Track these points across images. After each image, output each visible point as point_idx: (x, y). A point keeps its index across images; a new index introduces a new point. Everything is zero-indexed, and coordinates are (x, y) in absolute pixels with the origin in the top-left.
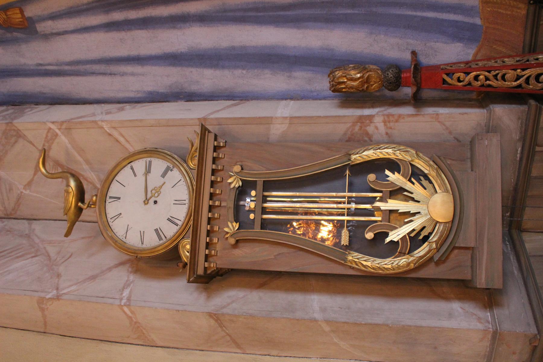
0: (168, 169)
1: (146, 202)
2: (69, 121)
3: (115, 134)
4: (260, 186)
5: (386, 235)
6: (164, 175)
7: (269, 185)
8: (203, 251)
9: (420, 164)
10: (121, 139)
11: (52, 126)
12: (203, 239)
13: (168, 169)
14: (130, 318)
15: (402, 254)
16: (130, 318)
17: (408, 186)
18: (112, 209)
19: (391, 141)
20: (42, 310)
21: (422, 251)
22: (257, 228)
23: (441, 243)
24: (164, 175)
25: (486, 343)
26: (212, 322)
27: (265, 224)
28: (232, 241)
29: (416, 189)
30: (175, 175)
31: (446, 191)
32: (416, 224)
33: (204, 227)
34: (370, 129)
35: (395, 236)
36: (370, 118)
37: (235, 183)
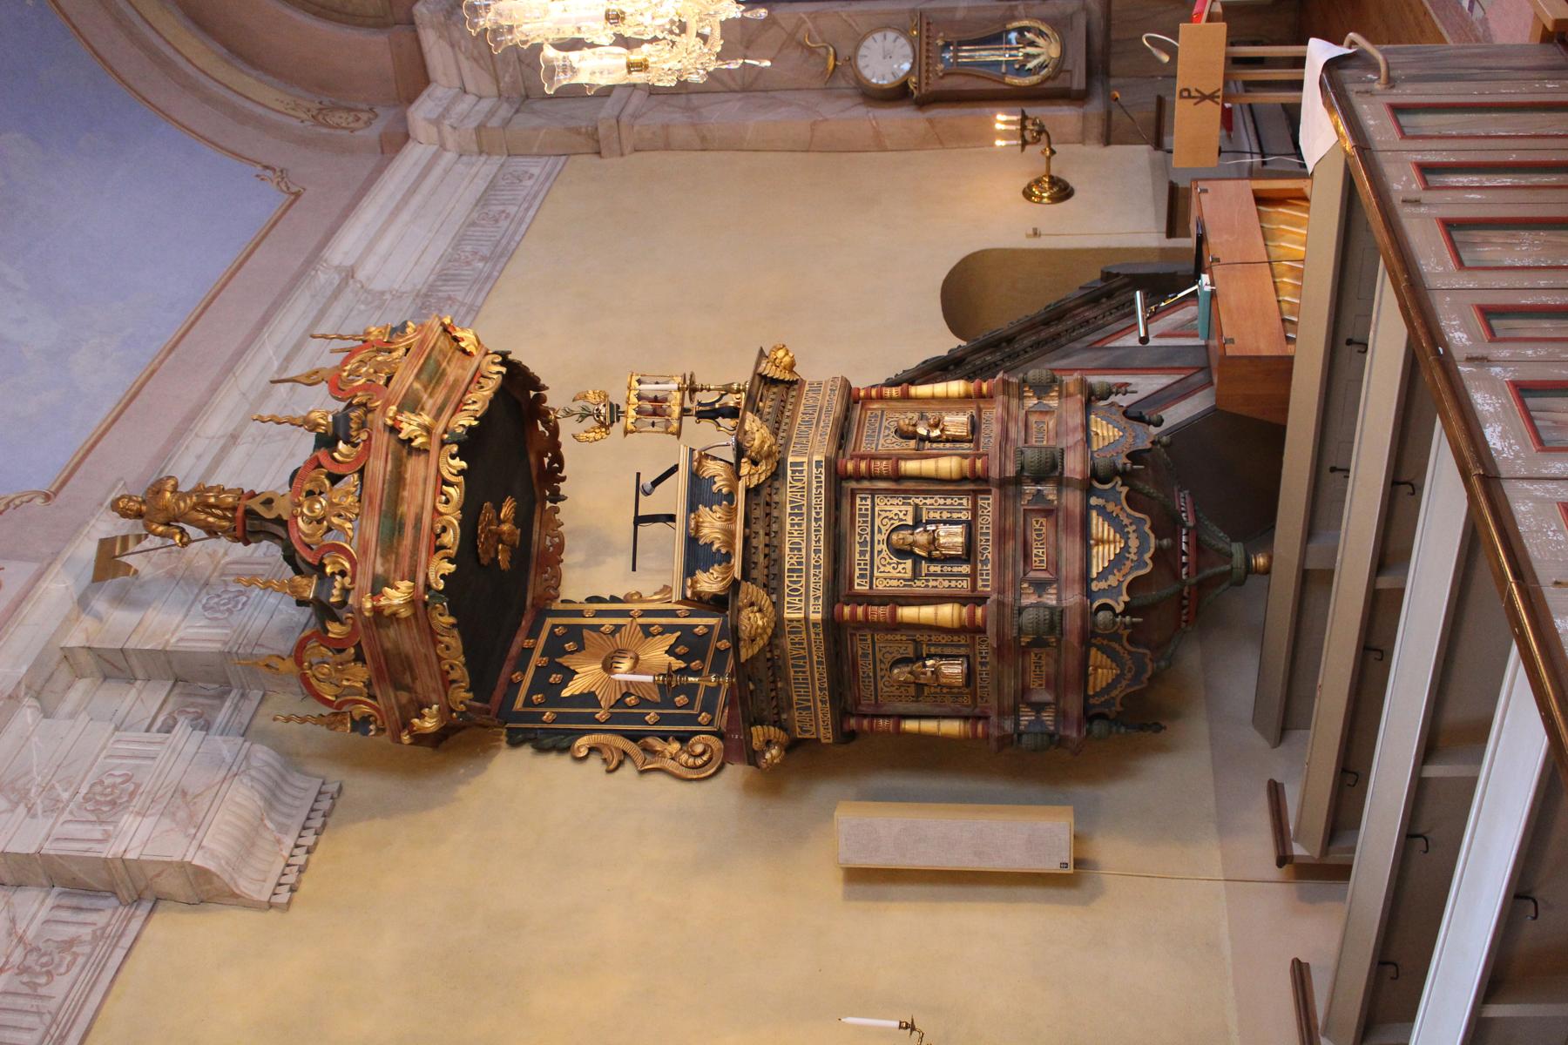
0: (897, 38)
1: (884, 58)
2: (817, 12)
3: (850, 21)
4: (955, 44)
5: (1025, 65)
6: (895, 41)
7: (961, 43)
8: (924, 81)
9: (1043, 28)
10: (854, 24)
11: (803, 16)
12: (924, 75)
13: (897, 38)
14: (874, 128)
15: (1034, 74)
16: (874, 128)
17: (1037, 40)
18: (861, 63)
19: (1027, 17)
20: (812, 130)
21: (1044, 72)
22: (955, 67)
23: (1055, 68)
24: (895, 41)
25: (1080, 124)
26: (927, 124)
27: (958, 64)
28: (941, 74)
29: (1040, 41)
30: (902, 41)
31: (1056, 40)
32: (1041, 59)
33: (924, 68)
34: (1016, 13)
35: (1030, 66)
36: (1016, 6)
37: (940, 43)
